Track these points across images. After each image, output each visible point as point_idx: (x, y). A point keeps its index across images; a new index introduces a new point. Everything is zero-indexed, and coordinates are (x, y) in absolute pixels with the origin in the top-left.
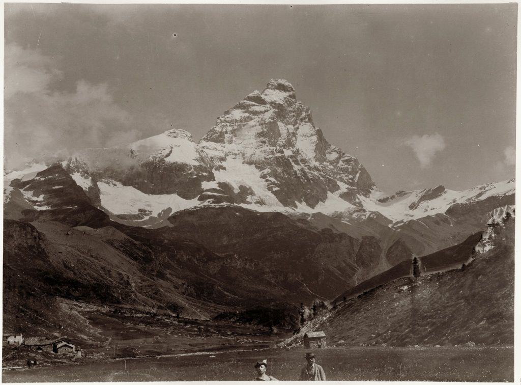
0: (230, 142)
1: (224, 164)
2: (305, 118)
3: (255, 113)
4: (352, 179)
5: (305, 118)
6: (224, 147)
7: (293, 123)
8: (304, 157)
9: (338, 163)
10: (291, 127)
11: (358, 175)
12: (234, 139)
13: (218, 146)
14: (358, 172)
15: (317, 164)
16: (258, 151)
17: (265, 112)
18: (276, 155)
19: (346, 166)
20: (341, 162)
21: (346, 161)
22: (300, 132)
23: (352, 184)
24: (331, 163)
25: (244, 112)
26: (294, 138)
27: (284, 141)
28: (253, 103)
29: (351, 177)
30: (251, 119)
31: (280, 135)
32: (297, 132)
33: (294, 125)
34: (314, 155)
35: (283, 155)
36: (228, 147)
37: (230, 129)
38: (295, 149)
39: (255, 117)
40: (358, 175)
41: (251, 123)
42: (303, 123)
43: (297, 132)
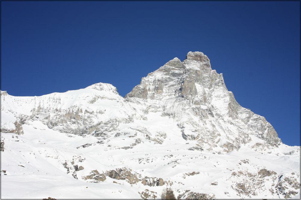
0: (152, 98)
1: (146, 116)
2: (219, 83)
3: (174, 75)
4: (262, 135)
5: (219, 83)
6: (147, 101)
7: (209, 87)
8: (218, 112)
9: (248, 121)
10: (207, 90)
11: (266, 131)
12: (155, 96)
13: (141, 100)
14: (265, 129)
15: (230, 119)
16: (177, 104)
17: (183, 74)
18: (192, 106)
19: (255, 124)
20: (251, 121)
21: (254, 120)
22: (214, 94)
23: (263, 138)
24: (242, 120)
25: (166, 74)
26: (210, 98)
27: (200, 98)
28: (173, 67)
29: (260, 133)
30: (172, 80)
31: (196, 93)
32: (213, 94)
33: (209, 88)
34: (227, 111)
35: (199, 106)
36: (150, 102)
37: (152, 87)
38: (210, 106)
39: (175, 78)
40: (266, 131)
41: (171, 83)
42: (217, 87)
43: (213, 94)
